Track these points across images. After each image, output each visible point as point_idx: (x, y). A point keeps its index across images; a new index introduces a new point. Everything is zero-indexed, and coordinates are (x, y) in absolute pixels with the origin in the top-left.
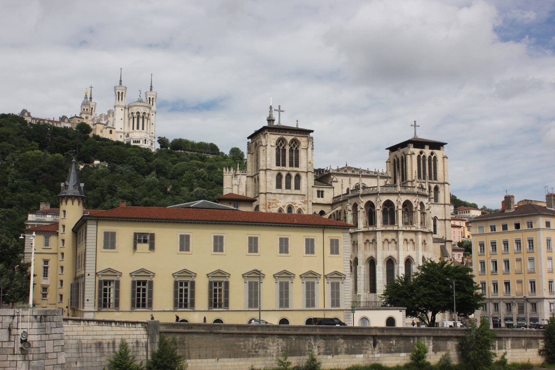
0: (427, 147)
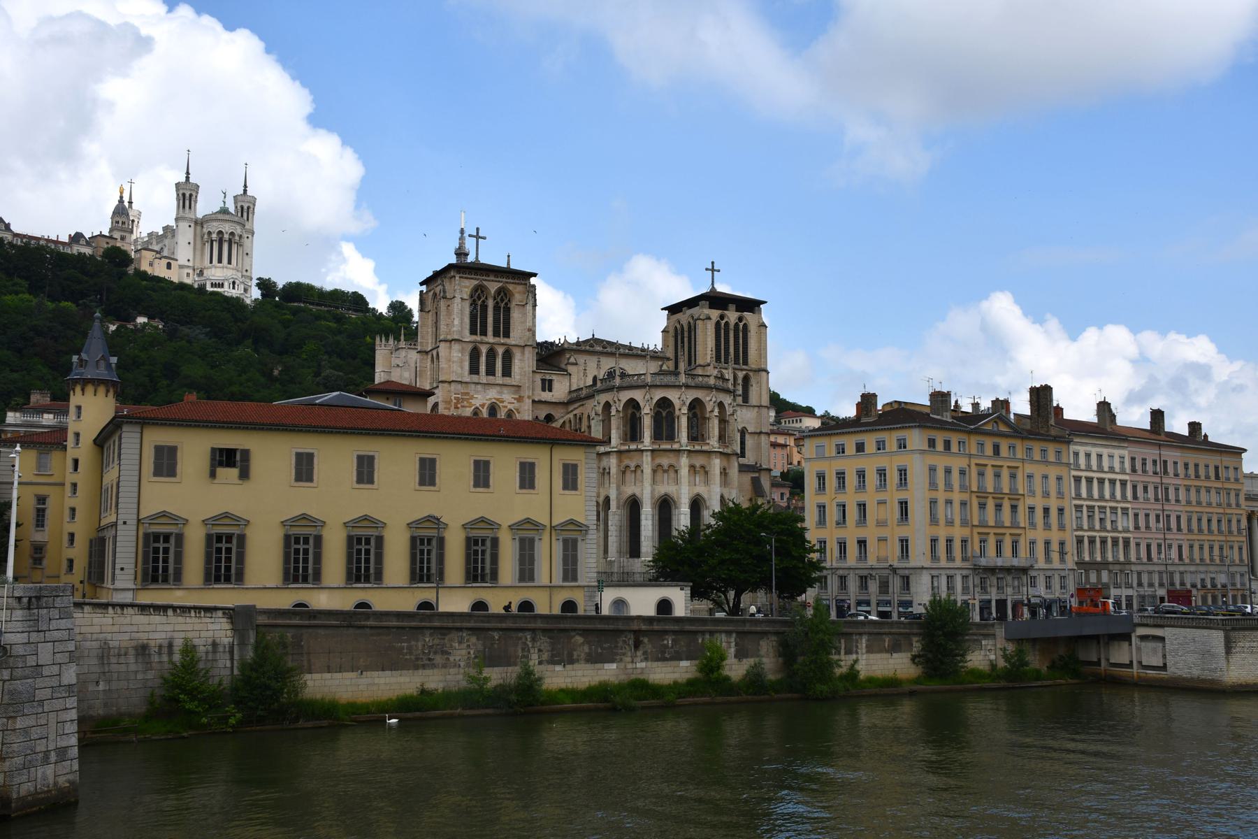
0: (732, 307)
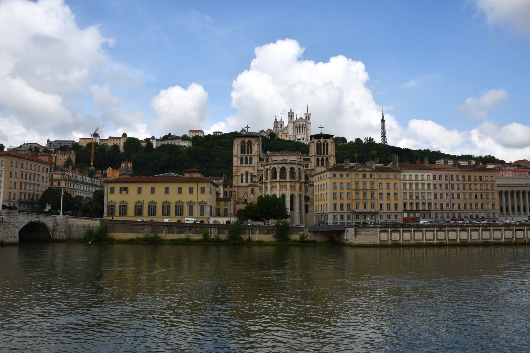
0: (322, 138)
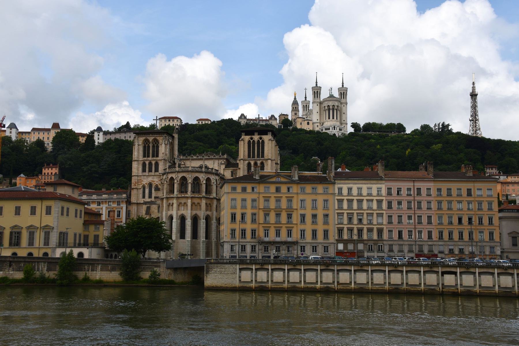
0: (256, 134)
